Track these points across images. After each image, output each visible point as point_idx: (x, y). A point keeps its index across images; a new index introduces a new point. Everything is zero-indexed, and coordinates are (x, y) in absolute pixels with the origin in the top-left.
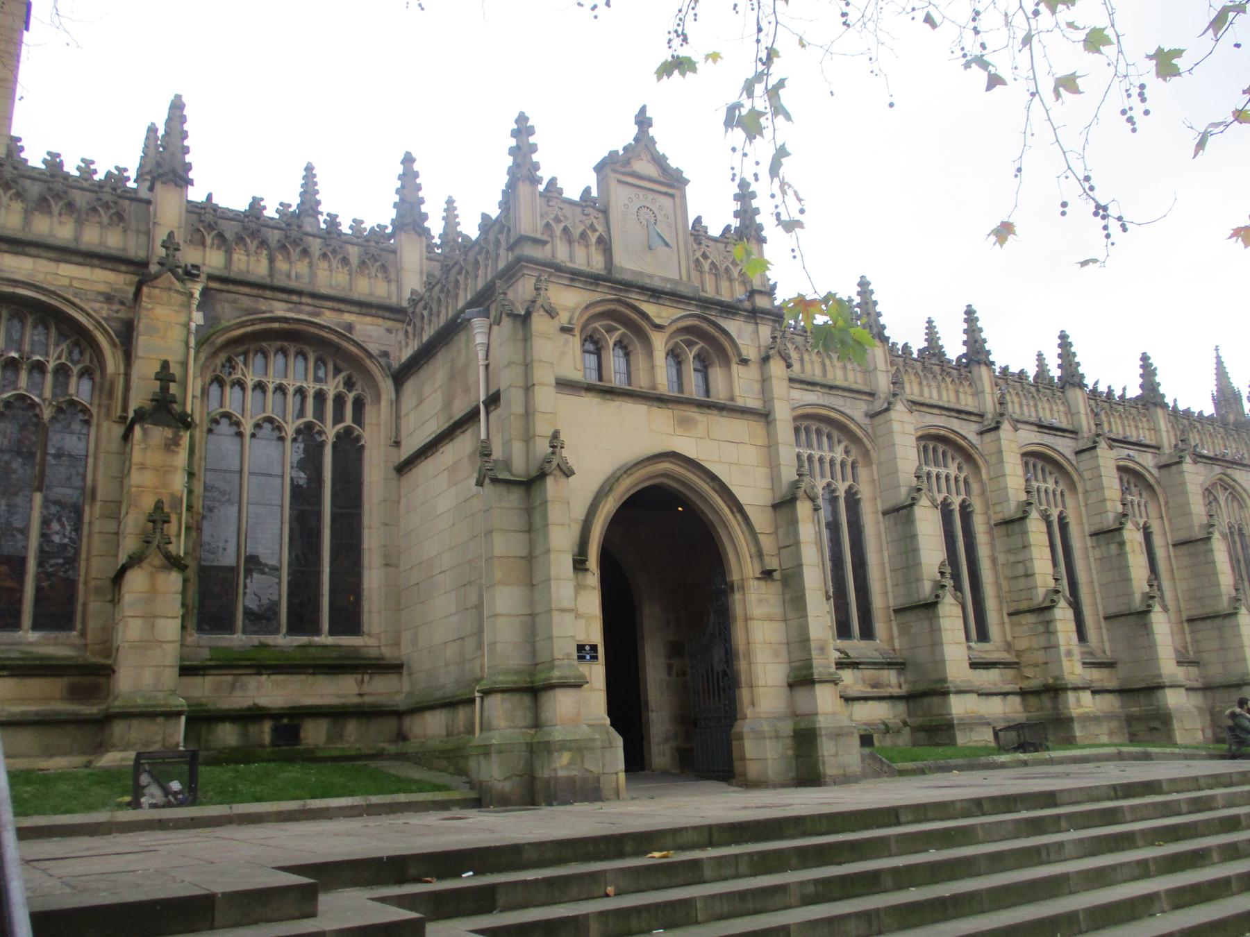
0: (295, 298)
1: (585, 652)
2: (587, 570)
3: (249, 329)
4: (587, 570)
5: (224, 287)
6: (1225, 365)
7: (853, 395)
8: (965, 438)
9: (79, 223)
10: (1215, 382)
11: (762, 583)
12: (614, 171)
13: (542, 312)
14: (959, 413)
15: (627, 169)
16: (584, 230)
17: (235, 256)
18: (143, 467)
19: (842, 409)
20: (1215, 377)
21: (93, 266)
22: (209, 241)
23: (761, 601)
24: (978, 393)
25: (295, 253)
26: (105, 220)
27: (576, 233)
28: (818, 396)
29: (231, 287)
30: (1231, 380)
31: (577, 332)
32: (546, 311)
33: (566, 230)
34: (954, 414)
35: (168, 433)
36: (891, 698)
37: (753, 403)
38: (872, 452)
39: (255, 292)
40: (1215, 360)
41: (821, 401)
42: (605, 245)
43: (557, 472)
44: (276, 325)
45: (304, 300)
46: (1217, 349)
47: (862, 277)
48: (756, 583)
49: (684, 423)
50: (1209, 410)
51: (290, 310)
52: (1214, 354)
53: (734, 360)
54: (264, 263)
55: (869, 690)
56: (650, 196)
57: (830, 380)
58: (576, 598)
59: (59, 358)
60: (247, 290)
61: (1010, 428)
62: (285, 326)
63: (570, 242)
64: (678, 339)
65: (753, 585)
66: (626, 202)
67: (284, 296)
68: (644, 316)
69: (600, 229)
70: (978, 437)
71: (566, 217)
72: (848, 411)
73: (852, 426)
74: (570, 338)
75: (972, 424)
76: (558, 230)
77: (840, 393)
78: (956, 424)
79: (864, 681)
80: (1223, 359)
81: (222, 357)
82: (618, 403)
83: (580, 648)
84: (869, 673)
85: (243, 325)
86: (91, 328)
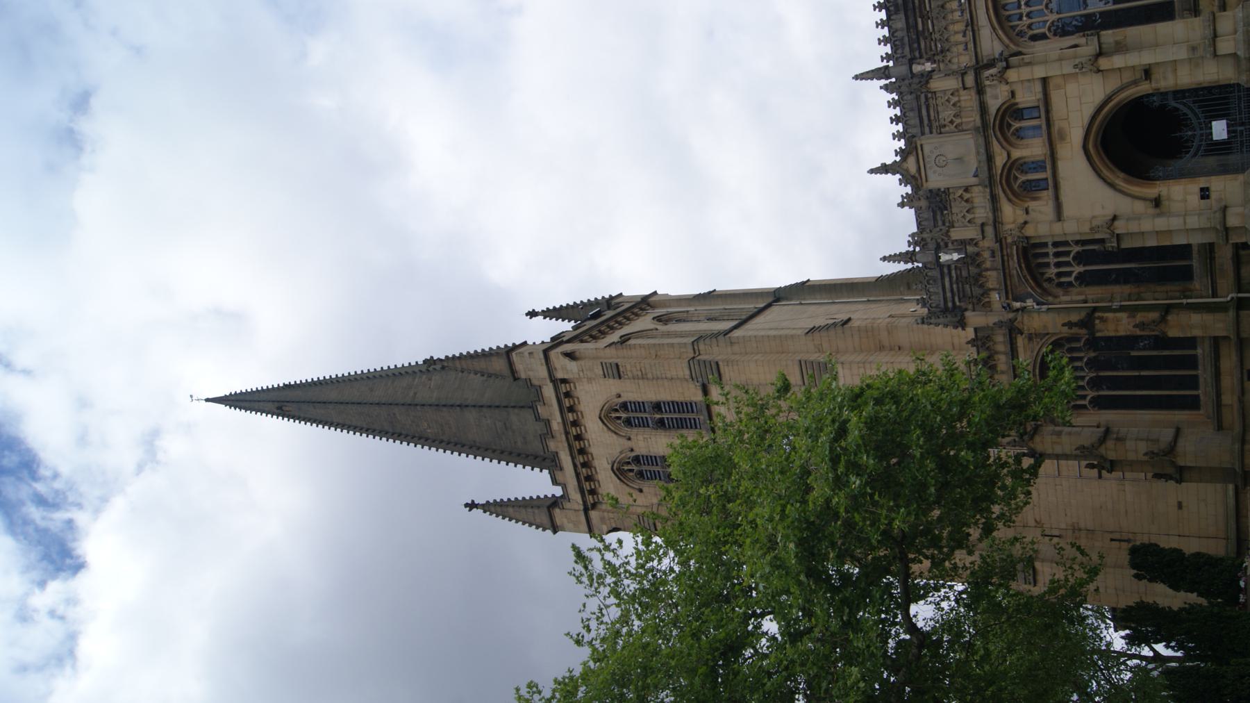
0: (1006, 258)
1: (1205, 194)
2: (1159, 195)
4: (1159, 195)
5: (1010, 292)
9: (997, 353)
11: (1153, 77)
12: (922, 185)
13: (1023, 231)
15: (917, 175)
17: (991, 287)
18: (1116, 331)
22: (987, 300)
23: (1165, 78)
25: (979, 260)
26: (991, 343)
27: (968, 206)
29: (1009, 288)
31: (1026, 205)
33: (968, 212)
35: (1097, 322)
37: (1038, 87)
39: (1008, 278)
43: (1112, 228)
44: (1023, 265)
45: (1005, 253)
48: (1153, 82)
49: (1062, 137)
51: (1012, 259)
53: (1013, 101)
54: (989, 273)
56: (927, 160)
62: (1022, 261)
63: (973, 208)
64: (1009, 135)
65: (1154, 85)
67: (1006, 263)
68: (1005, 165)
69: (960, 192)
74: (1030, 209)
76: (969, 216)
81: (1046, 285)
82: (1061, 180)
83: (1203, 197)
85: (1027, 280)
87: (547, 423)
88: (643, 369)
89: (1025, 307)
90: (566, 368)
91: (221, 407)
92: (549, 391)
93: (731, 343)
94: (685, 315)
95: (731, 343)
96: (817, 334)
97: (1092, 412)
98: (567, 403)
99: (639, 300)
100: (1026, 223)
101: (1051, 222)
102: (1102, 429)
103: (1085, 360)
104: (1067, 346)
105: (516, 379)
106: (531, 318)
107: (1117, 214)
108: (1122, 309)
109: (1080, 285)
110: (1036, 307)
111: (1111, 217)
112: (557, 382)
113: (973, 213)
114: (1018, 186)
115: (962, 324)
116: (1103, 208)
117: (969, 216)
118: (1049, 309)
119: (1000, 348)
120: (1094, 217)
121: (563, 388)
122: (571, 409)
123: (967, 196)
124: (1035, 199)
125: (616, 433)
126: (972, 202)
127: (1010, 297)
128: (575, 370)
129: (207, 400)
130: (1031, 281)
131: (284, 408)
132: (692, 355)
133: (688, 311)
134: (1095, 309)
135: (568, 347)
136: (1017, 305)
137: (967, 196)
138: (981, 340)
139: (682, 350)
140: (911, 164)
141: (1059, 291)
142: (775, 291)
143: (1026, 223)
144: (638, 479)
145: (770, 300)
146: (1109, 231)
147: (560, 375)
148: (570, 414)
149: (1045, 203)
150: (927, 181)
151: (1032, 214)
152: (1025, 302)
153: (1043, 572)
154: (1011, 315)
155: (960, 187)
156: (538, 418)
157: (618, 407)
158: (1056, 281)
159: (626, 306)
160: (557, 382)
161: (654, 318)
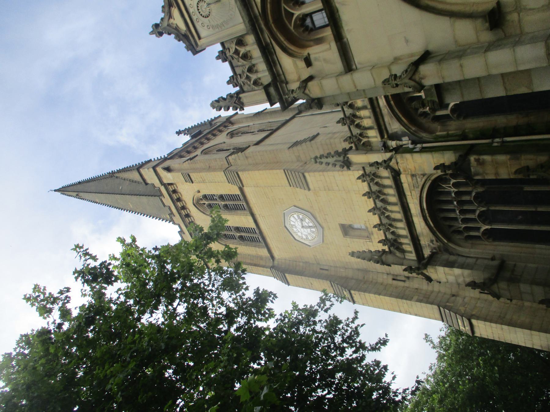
3: (401, 116)
13: (307, 91)
16: (242, 58)
18: (497, 174)
21: (401, 183)
27: (247, 64)
29: (383, 127)
32: (305, 89)
42: (240, 42)
43: (417, 77)
44: (392, 102)
56: (191, 10)
58: (530, 9)
59: (450, 187)
60: (381, 121)
66: (206, 27)
71: (243, 72)
74: (312, 57)
76: (254, 77)
86: (430, 181)
87: (170, 208)
88: (202, 177)
89: (401, 146)
90: (168, 177)
91: (58, 194)
92: (163, 189)
93: (246, 157)
94: (247, 128)
95: (246, 157)
96: (295, 148)
97: (487, 243)
98: (175, 197)
99: (225, 120)
100: (311, 78)
101: (340, 75)
102: (496, 263)
103: (473, 194)
104: (453, 181)
105: (147, 184)
106: (178, 135)
107: (431, 48)
108: (504, 149)
109: (458, 118)
110: (411, 146)
111: (416, 58)
112: (166, 186)
113: (257, 72)
114: (294, 28)
115: (347, 164)
116: (407, 41)
117: (254, 77)
118: (423, 148)
119: (388, 182)
120: (396, 60)
121: (171, 188)
122: (179, 200)
123: (242, 50)
124: (319, 41)
125: (204, 213)
126: (251, 58)
127: (386, 137)
128: (172, 179)
129: (55, 191)
130: (403, 119)
131: (79, 195)
132: (227, 166)
133: (249, 126)
134: (471, 150)
135: (166, 164)
136: (393, 144)
137: (242, 50)
138: (369, 176)
139: (222, 163)
140: (178, 20)
141: (436, 126)
142: (298, 107)
143: (311, 78)
144: (224, 238)
145: (297, 112)
146: (412, 83)
147: (165, 181)
148: (178, 203)
149: (328, 46)
150: (200, 38)
151: (317, 65)
152: (401, 140)
153: (478, 326)
154: (388, 155)
155: (231, 41)
156: (164, 205)
157: (201, 198)
158: (432, 115)
159: (218, 124)
160: (166, 186)
161: (227, 134)
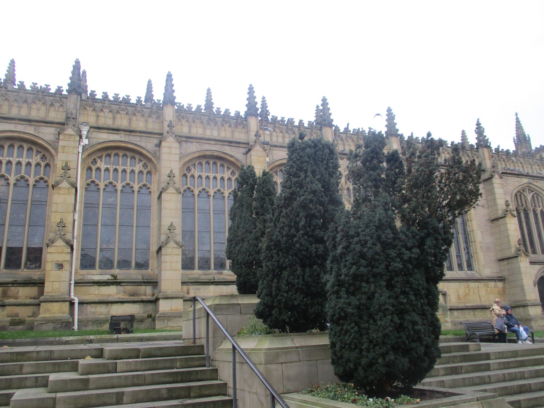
6: (521, 122)
7: (147, 135)
8: (232, 156)
10: (515, 132)
14: (230, 143)
19: (139, 143)
20: (515, 129)
24: (248, 132)
28: (121, 137)
30: (524, 131)
34: (227, 144)
36: (142, 302)
38: (157, 166)
40: (515, 121)
41: (123, 139)
46: (516, 115)
47: (169, 72)
50: (512, 148)
52: (515, 117)
55: (128, 297)
57: (134, 127)
61: (261, 149)
70: (245, 156)
72: (143, 144)
73: (144, 152)
75: (241, 149)
77: (138, 134)
78: (228, 150)
79: (125, 292)
80: (520, 120)
84: (129, 288)
